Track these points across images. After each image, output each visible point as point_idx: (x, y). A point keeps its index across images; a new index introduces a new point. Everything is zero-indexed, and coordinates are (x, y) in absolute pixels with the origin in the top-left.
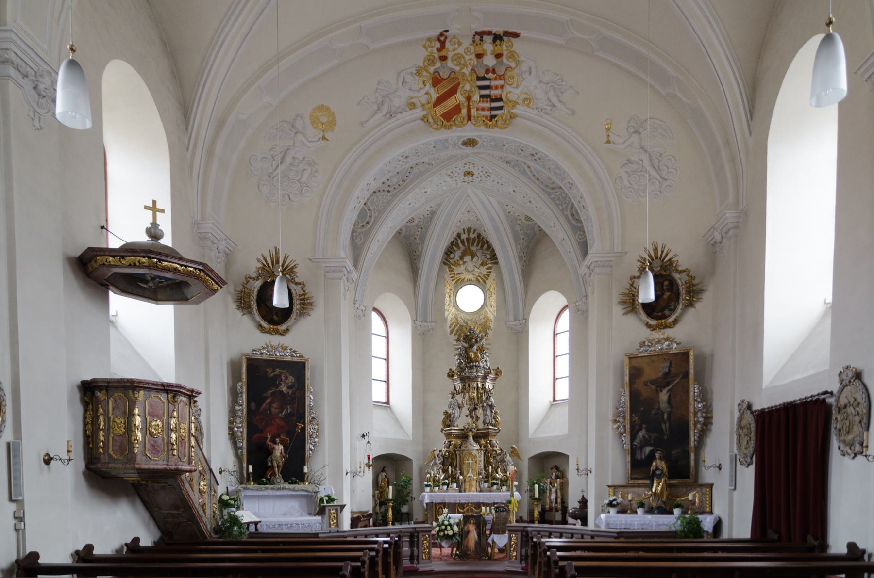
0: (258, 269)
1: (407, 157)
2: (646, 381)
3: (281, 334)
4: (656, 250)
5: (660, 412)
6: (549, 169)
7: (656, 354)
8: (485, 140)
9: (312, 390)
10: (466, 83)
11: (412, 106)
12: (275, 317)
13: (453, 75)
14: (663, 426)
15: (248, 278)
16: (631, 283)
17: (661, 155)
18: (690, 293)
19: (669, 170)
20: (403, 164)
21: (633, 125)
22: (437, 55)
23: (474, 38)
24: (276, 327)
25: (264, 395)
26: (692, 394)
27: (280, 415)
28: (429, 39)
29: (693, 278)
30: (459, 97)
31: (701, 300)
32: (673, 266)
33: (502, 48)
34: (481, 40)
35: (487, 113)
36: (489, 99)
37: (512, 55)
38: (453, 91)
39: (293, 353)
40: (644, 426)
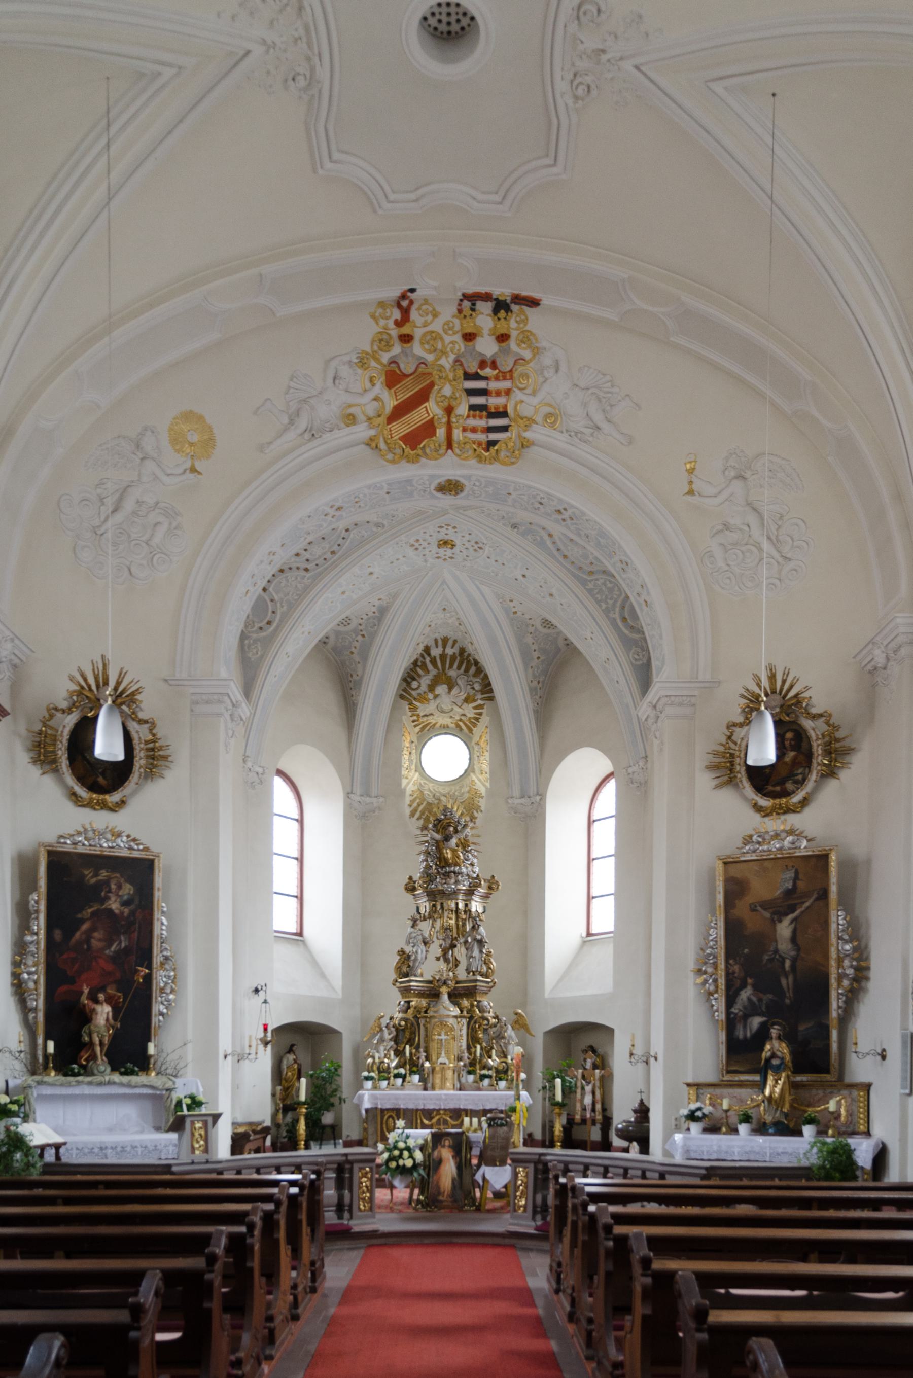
0: (71, 694)
1: (339, 509)
2: (753, 904)
3: (112, 810)
4: (772, 677)
5: (777, 956)
6: (587, 537)
7: (772, 856)
8: (477, 484)
10: (445, 384)
11: (351, 419)
12: (101, 780)
13: (422, 368)
14: (784, 982)
15: (53, 708)
16: (729, 734)
17: (781, 517)
18: (830, 753)
19: (796, 544)
20: (334, 520)
21: (733, 464)
22: (394, 332)
23: (460, 305)
24: (101, 797)
25: (79, 916)
26: (833, 927)
27: (107, 952)
28: (382, 304)
29: (836, 728)
30: (433, 408)
31: (850, 766)
32: (802, 706)
33: (508, 324)
34: (473, 310)
35: (482, 437)
36: (484, 413)
37: (527, 338)
38: (422, 397)
40: (749, 981)
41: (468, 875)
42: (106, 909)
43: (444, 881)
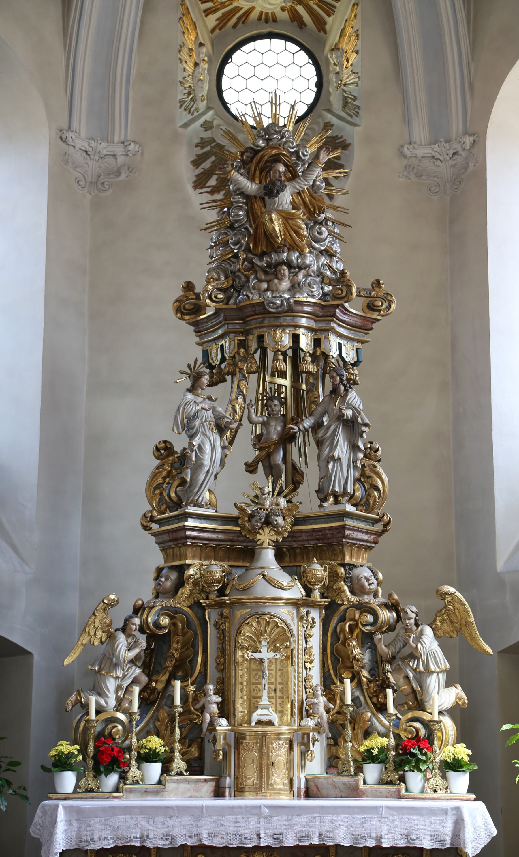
41: (320, 274)
43: (265, 286)
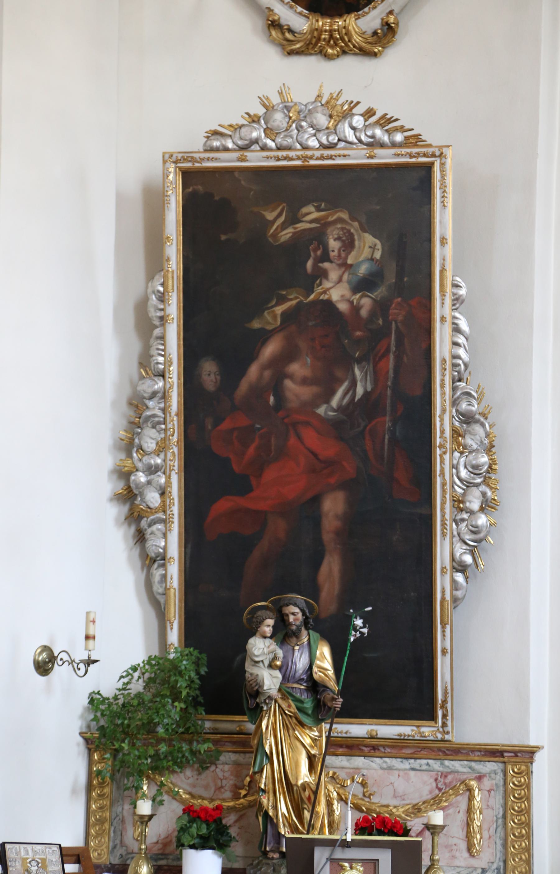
9: (462, 292)
25: (256, 324)
27: (321, 410)
39: (378, 132)
42: (317, 302)
